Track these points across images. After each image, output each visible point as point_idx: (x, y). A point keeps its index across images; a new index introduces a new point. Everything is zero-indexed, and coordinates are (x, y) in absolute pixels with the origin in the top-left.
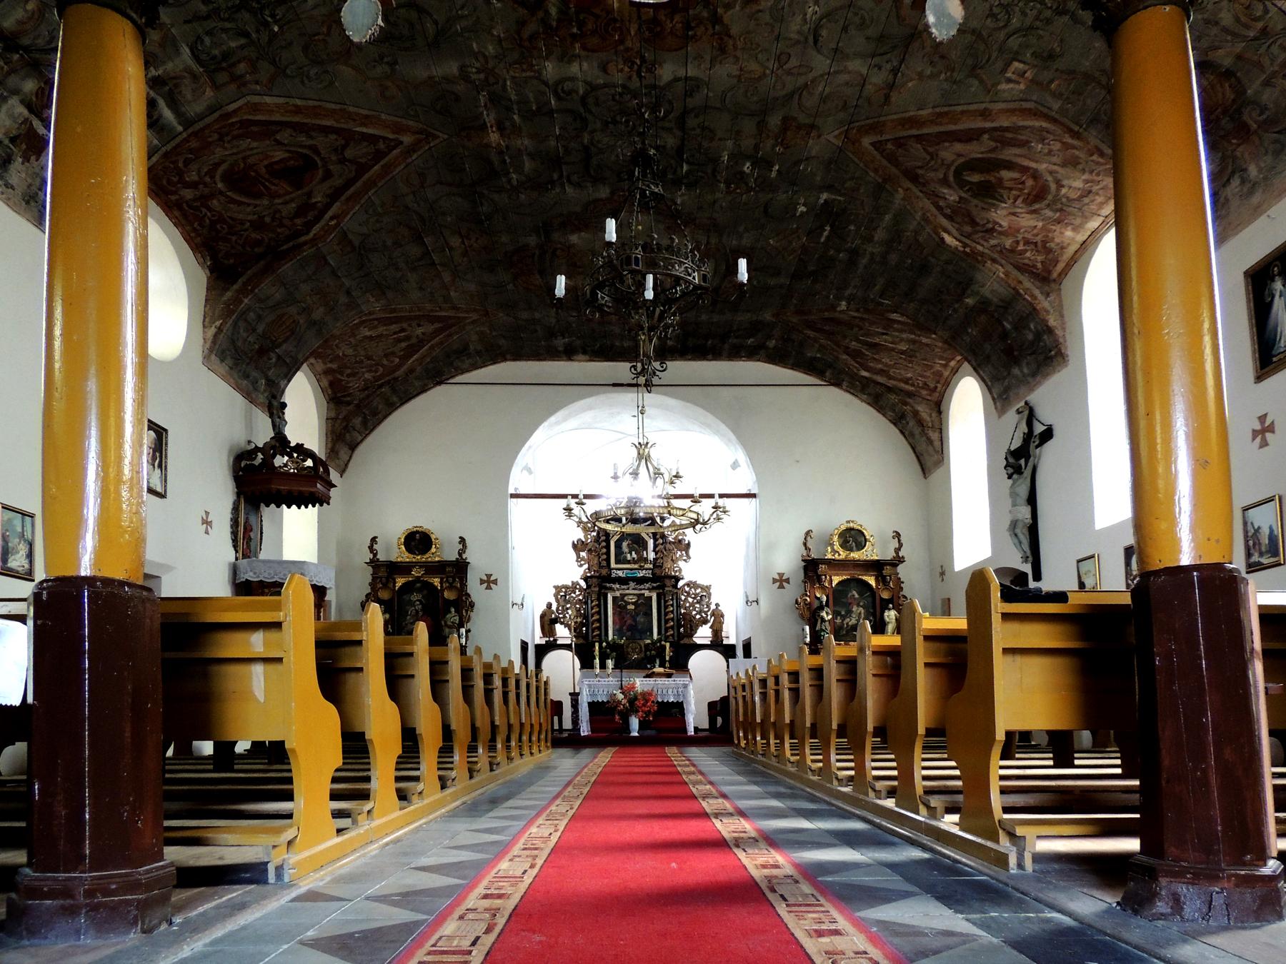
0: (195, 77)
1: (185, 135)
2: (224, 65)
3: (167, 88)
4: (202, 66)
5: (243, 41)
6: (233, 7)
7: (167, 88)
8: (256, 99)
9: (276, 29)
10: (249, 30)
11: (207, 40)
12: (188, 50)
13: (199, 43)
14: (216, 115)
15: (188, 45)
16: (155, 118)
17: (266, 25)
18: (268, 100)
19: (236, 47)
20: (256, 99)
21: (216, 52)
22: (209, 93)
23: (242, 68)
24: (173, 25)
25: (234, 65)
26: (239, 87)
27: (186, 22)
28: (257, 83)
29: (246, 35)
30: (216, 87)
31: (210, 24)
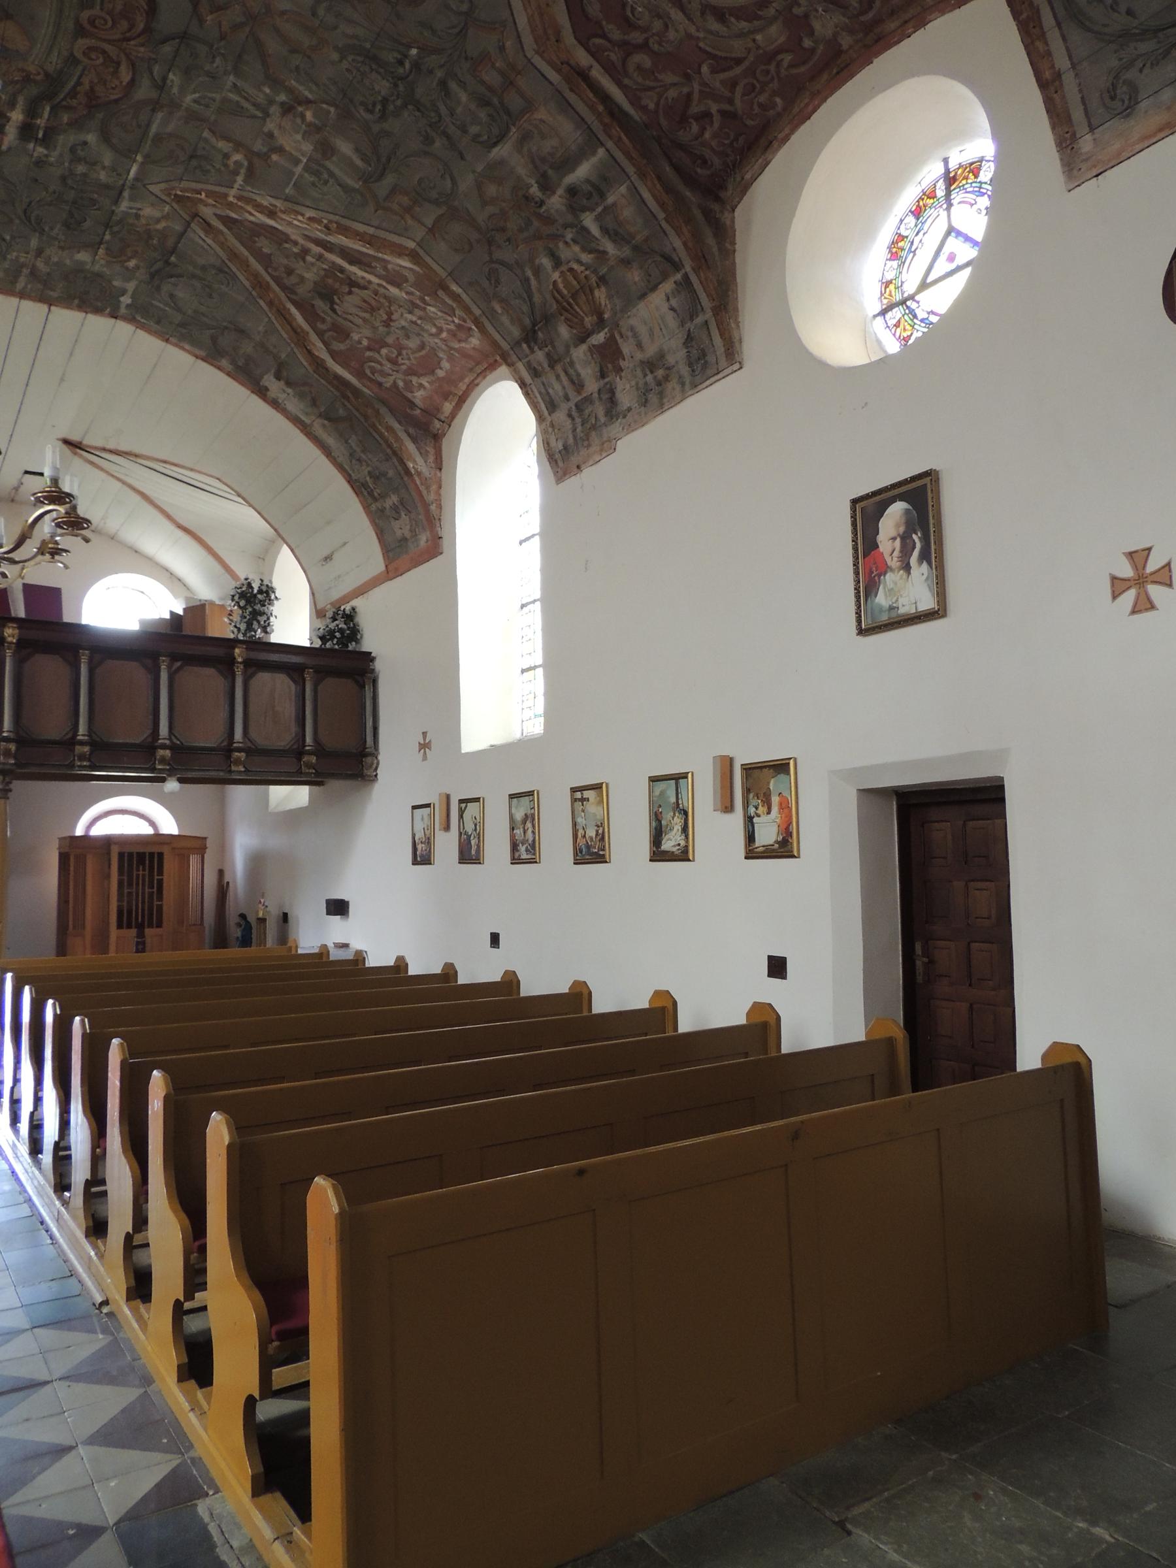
0: (525, 137)
1: (610, 144)
2: (495, 101)
3: (550, 172)
4: (508, 129)
5: (453, 85)
6: (419, 110)
7: (550, 172)
8: (528, 40)
9: (414, 51)
10: (435, 84)
11: (474, 129)
12: (495, 150)
13: (481, 139)
14: (572, 98)
15: (489, 152)
16: (590, 188)
17: (416, 66)
18: (522, 21)
19: (465, 91)
20: (528, 40)
21: (483, 115)
22: (541, 114)
23: (491, 77)
24: (474, 172)
25: (490, 88)
26: (519, 73)
27: (462, 158)
28: (502, 48)
29: (443, 84)
30: (530, 106)
31: (452, 129)
